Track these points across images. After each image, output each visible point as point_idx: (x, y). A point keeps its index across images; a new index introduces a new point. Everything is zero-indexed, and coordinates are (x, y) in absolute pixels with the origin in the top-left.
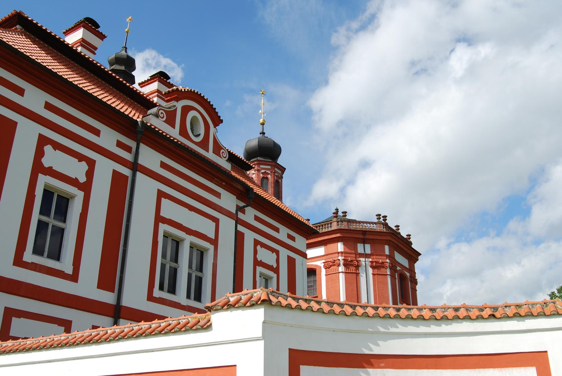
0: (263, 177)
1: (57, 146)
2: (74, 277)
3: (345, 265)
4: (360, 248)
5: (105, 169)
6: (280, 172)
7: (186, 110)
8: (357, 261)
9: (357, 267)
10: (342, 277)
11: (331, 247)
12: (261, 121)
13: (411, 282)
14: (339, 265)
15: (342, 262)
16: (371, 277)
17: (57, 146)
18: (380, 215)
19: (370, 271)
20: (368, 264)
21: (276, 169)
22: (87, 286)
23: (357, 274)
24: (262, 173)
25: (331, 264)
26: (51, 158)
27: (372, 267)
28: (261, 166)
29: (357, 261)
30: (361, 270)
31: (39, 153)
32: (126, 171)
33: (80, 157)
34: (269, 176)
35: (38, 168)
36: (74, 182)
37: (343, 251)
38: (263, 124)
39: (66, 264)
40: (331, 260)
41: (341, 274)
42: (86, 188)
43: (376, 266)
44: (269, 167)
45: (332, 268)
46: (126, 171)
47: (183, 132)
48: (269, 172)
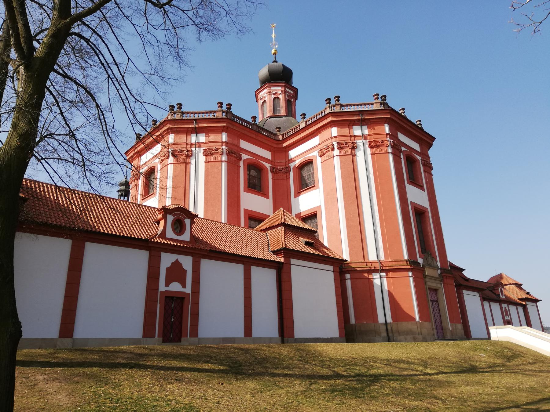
0: (275, 98)
3: (340, 148)
4: (357, 131)
6: (292, 92)
8: (353, 143)
9: (354, 148)
10: (337, 160)
11: (325, 134)
12: (273, 51)
13: (424, 165)
14: (333, 149)
15: (336, 146)
16: (369, 157)
18: (378, 95)
19: (369, 151)
21: (287, 89)
23: (353, 156)
24: (274, 94)
25: (326, 151)
27: (371, 147)
28: (272, 88)
29: (353, 143)
34: (280, 96)
37: (336, 135)
38: (275, 54)
40: (326, 147)
41: (335, 158)
43: (374, 145)
44: (280, 88)
45: (326, 154)
48: (280, 92)
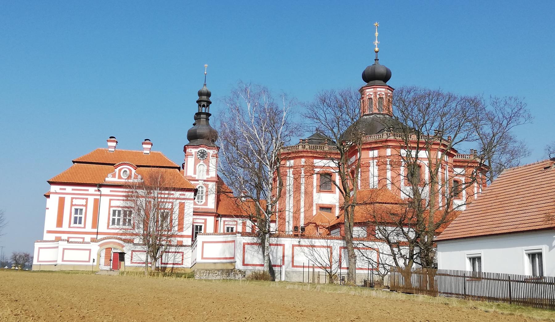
1: (76, 198)
2: (85, 227)
5: (91, 200)
7: (120, 170)
17: (76, 198)
19: (376, 168)
20: (375, 163)
22: (89, 228)
26: (75, 202)
30: (371, 169)
31: (72, 202)
32: (99, 197)
33: (83, 199)
35: (72, 205)
36: (82, 205)
39: (82, 225)
42: (86, 206)
46: (99, 197)
47: (120, 177)
